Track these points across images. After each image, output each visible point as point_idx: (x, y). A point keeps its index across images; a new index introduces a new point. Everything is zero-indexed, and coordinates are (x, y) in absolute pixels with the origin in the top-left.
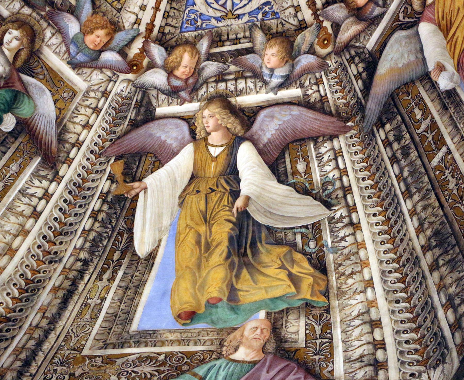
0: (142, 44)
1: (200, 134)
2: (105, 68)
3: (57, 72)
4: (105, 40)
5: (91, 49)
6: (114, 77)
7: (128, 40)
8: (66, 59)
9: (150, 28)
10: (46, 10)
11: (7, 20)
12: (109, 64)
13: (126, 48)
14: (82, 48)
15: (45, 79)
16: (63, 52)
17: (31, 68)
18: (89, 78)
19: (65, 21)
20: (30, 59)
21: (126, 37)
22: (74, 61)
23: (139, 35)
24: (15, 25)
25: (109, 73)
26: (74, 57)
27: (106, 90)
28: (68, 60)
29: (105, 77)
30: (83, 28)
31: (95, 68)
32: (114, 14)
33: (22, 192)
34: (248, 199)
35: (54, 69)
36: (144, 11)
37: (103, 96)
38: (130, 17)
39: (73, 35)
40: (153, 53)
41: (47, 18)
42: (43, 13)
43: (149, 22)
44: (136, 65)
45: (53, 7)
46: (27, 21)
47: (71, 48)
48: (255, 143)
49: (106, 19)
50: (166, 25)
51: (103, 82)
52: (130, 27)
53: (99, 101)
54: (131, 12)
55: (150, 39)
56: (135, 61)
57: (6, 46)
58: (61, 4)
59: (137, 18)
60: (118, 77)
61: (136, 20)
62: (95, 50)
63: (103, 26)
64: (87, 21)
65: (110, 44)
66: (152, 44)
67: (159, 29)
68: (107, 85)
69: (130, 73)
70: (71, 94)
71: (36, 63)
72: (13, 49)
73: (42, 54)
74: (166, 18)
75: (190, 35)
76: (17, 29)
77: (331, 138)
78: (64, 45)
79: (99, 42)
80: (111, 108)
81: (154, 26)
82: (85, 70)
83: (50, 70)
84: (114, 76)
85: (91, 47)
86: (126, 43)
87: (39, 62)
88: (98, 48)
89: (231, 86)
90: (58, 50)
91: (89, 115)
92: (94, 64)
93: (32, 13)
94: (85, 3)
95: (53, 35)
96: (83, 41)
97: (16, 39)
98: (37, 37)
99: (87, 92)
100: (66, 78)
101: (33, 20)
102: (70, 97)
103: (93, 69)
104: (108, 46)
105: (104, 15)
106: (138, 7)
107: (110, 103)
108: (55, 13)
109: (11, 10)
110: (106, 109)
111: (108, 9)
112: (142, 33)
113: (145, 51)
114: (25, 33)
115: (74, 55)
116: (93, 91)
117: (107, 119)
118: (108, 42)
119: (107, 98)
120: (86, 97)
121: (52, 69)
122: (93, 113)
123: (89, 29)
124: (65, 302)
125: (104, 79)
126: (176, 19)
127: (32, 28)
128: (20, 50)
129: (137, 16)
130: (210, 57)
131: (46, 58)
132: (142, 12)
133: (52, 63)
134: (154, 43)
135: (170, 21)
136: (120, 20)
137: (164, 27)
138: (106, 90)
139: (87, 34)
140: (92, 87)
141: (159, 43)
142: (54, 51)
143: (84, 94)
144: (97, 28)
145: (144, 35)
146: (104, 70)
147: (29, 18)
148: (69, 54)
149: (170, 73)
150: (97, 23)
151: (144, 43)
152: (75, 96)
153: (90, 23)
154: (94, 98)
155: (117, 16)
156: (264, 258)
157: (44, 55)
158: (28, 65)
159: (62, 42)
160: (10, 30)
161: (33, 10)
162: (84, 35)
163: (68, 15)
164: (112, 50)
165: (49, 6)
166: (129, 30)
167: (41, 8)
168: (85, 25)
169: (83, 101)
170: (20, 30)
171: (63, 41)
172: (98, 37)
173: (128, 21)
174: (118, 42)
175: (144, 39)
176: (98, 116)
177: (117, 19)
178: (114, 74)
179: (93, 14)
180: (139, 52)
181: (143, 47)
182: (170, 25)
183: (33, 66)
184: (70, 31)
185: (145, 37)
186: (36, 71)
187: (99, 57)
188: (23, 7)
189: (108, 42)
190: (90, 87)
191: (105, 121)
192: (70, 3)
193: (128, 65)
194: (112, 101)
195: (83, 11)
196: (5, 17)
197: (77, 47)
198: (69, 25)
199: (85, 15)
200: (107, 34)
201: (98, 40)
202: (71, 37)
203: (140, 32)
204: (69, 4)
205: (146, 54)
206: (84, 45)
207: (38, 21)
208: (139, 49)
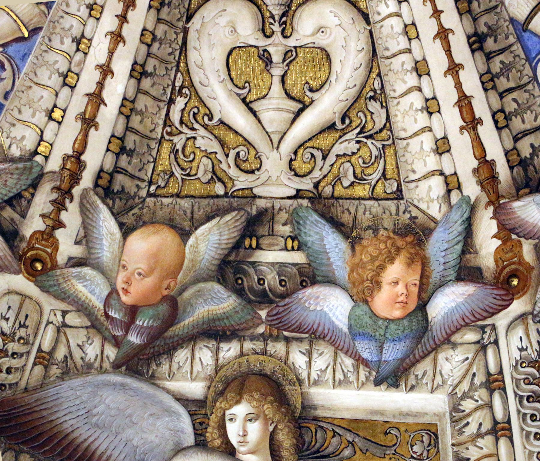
0: (494, 222)
2: (454, 333)
3: (369, 417)
4: (414, 278)
5: (399, 319)
6: (486, 336)
7: (460, 238)
8: (367, 378)
10: (260, 318)
11: (210, 398)
12: (456, 317)
13: (468, 256)
14: (382, 333)
15: (357, 450)
16: (352, 370)
17: (318, 451)
18: (438, 379)
19: (312, 308)
20: (301, 436)
21: (451, 237)
22: (386, 369)
23: (473, 209)
24: (230, 395)
25: (471, 336)
26: (380, 361)
27: (489, 374)
28: (372, 378)
29: (469, 351)
30: (354, 291)
31: (436, 348)
32: (393, 209)
35: (360, 416)
36: (448, 151)
37: (491, 392)
38: (430, 188)
39: (346, 321)
40: (531, 221)
41: (275, 333)
42: (261, 329)
43: (475, 163)
44: (513, 275)
45: (271, 302)
46: (244, 369)
47: (360, 350)
49: (385, 233)
50: (516, 139)
51: (471, 365)
52: (444, 208)
53: (491, 407)
54: (425, 177)
55: (503, 197)
56: (504, 268)
57: (242, 449)
58: (281, 281)
59: (446, 177)
60: (494, 327)
61: (447, 184)
62: (409, 315)
63: (390, 252)
64: (352, 271)
65: (428, 277)
66: (516, 204)
67: (508, 161)
68: (482, 363)
69: (512, 300)
70: (426, 439)
71: (319, 434)
72: (259, 443)
73: (315, 408)
74: (507, 126)
76: (238, 402)
78: (342, 355)
79: (405, 292)
80: (525, 402)
81: (491, 165)
82: (419, 370)
83: (354, 425)
84: (484, 332)
85: (397, 313)
86: (459, 247)
87: (322, 428)
88: (413, 305)
90: (339, 376)
91: (492, 450)
92: (427, 342)
93: (242, 347)
94: (322, 240)
95: (309, 354)
96: (374, 315)
97: (250, 420)
98: (284, 383)
99: (455, 409)
100: (394, 416)
101: (253, 359)
102: (429, 445)
103: (433, 354)
104: (428, 284)
105: (376, 231)
106: (432, 154)
107: (516, 394)
108: (282, 309)
109: (202, 375)
110: (519, 412)
111: (374, 210)
112: (476, 200)
113: (512, 230)
114: (257, 396)
115: (375, 359)
116: (465, 396)
117: (534, 430)
118: (424, 276)
119: (504, 390)
120: (460, 419)
121: (356, 421)
122: (497, 440)
123: (367, 284)
125: (470, 356)
126: (528, 108)
127: (262, 375)
128: (272, 436)
129: (442, 173)
131: (329, 409)
132: (445, 156)
133: (348, 409)
134: (518, 197)
135: (517, 124)
136: (415, 212)
137: (515, 148)
138: (489, 374)
139: (372, 295)
140: (457, 390)
141: (527, 190)
142: (334, 383)
143: (452, 417)
144: (382, 268)
145: (485, 199)
146: (457, 338)
147: (244, 359)
148: (366, 363)
150: (373, 259)
151: (496, 216)
152: (436, 436)
153: (360, 271)
154: (476, 409)
155: (402, 208)
157: (322, 406)
158: (307, 450)
159: (335, 353)
160: (228, 412)
161: (239, 340)
162: (367, 302)
163: (309, 291)
164: (441, 285)
165: (263, 306)
166: (446, 216)
167: (251, 324)
168: (354, 283)
169: (461, 432)
170: (245, 396)
171: (337, 348)
172: (396, 283)
173: (432, 201)
174: (442, 261)
175: (491, 209)
176: (511, 439)
177: (408, 216)
178: (483, 328)
179: (353, 248)
180: (499, 242)
181: (501, 226)
182: (526, 133)
183: (318, 445)
184: (334, 319)
185: (491, 203)
186: (330, 449)
187: (427, 320)
188: (218, 349)
189: (422, 276)
190: (452, 395)
191: (532, 437)
192: (294, 265)
193: (498, 288)
194: (517, 387)
195: (329, 259)
196: (202, 398)
197: (371, 337)
198: (325, 309)
199: (339, 263)
200: (410, 263)
201: (400, 288)
202: (345, 329)
203: (473, 200)
204: (295, 270)
205: (517, 234)
206: (381, 322)
207: (264, 353)
208: (495, 236)
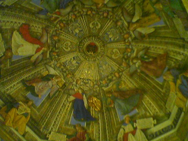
1: (134, 29)
9: (124, 43)
33: (154, 51)
34: (140, 17)
48: (132, 20)
75: (122, 37)
77: (126, 9)
89: (126, 28)
124: (167, 37)
130: (124, 33)
149: (128, 38)
156: (146, 10)
